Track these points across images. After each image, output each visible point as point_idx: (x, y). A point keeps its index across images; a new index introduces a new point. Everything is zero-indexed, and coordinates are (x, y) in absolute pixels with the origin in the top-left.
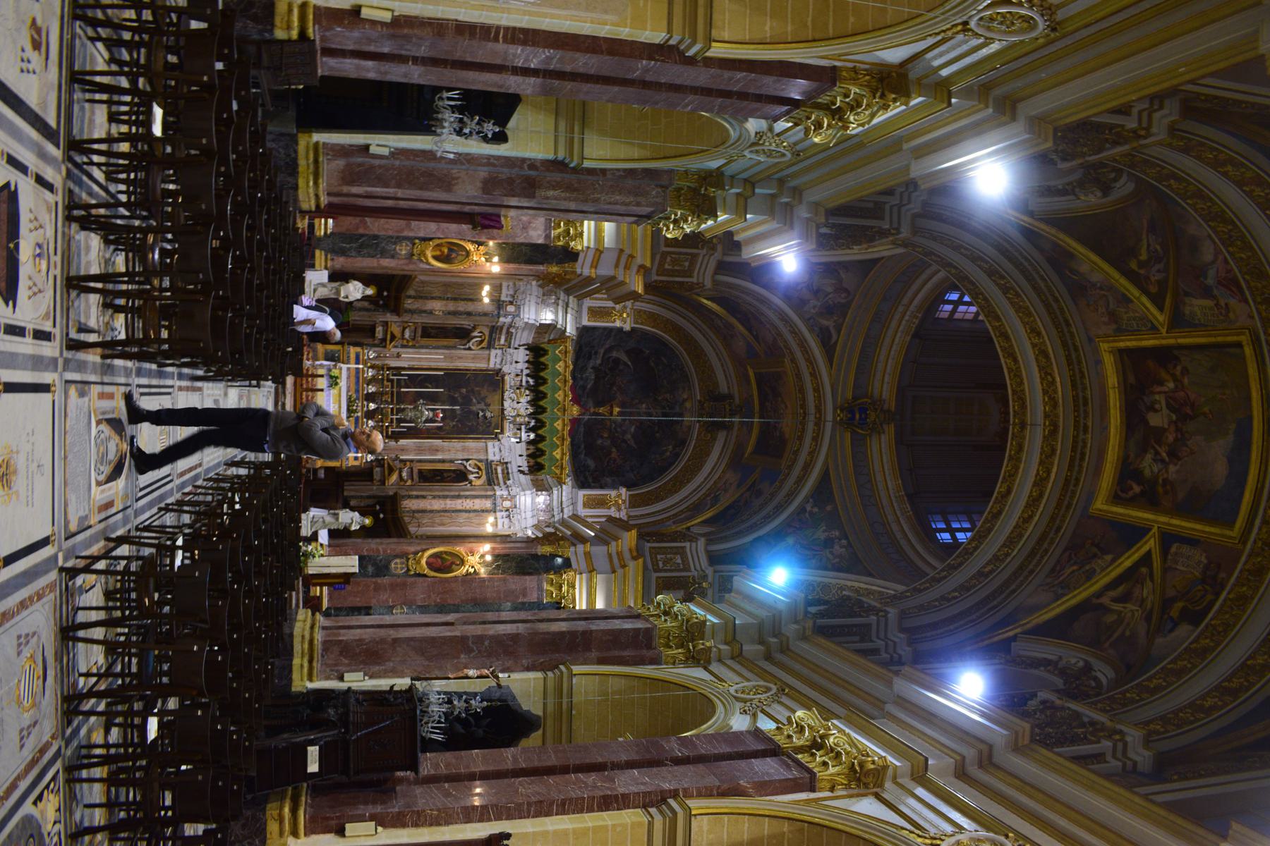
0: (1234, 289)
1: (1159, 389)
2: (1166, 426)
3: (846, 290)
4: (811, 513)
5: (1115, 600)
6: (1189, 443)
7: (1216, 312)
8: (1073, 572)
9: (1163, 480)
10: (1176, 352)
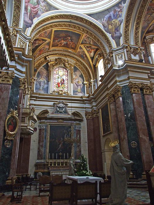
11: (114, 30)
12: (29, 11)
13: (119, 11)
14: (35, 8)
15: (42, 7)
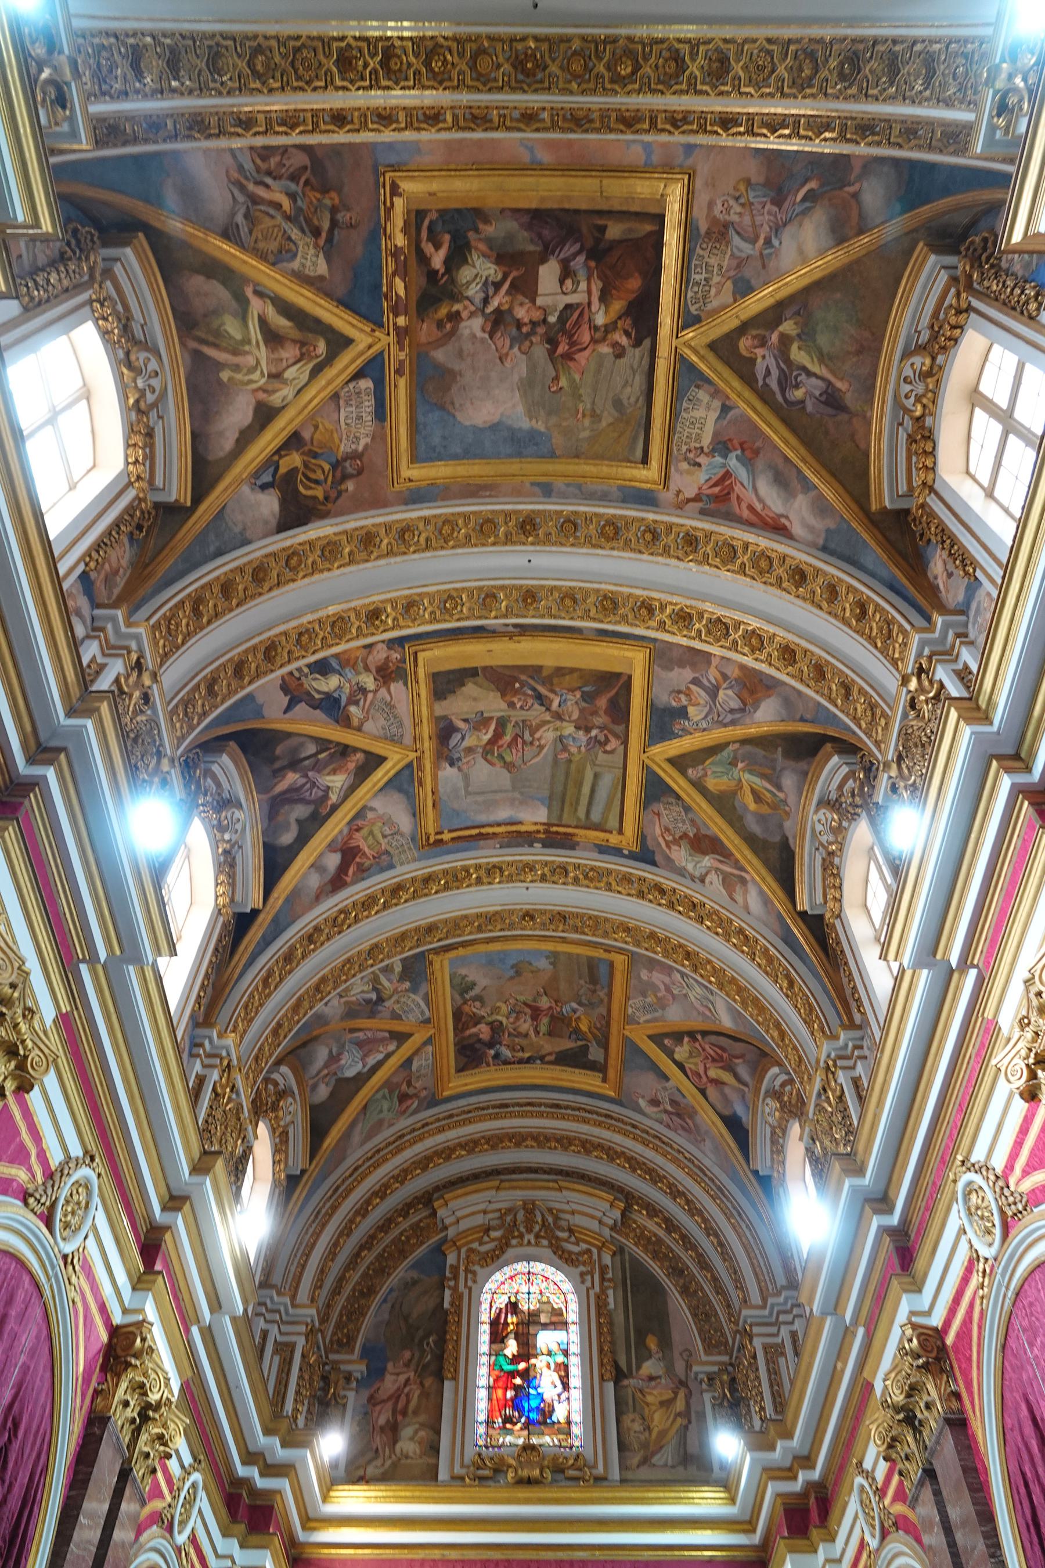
0: (717, 490)
1: (596, 286)
2: (539, 301)
6: (516, 350)
7: (693, 445)
8: (278, 206)
9: (458, 313)
10: (647, 343)
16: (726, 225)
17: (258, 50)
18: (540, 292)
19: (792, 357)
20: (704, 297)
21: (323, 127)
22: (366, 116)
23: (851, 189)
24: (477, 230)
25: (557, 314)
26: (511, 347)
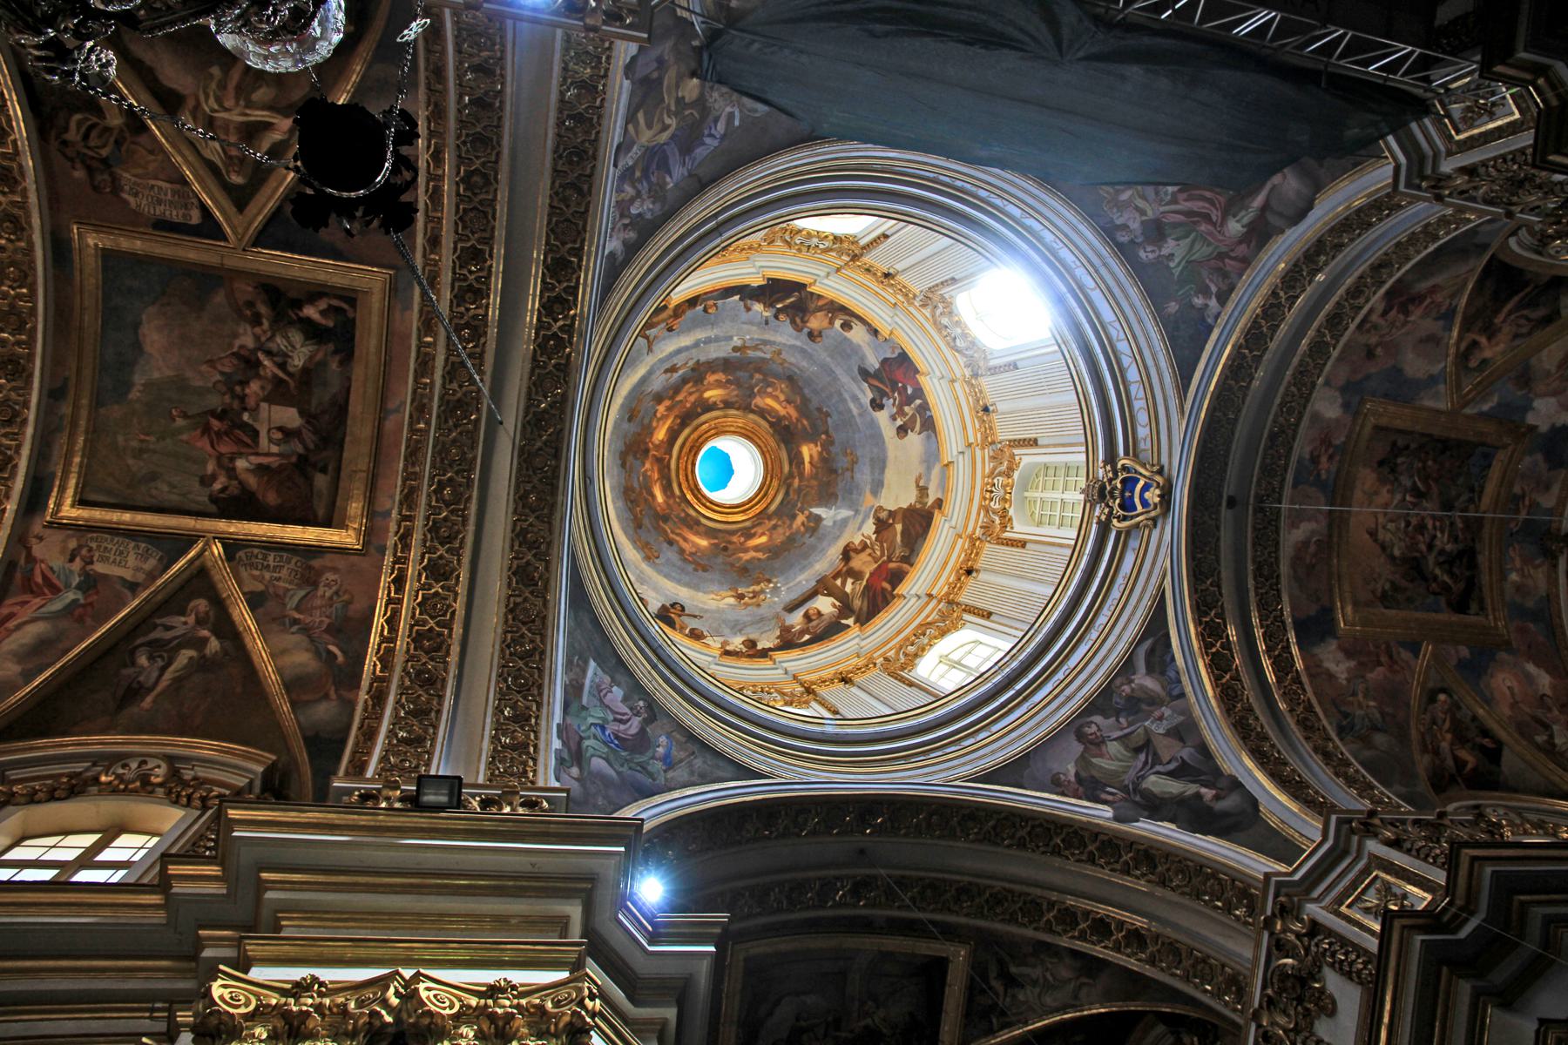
1: (273, 462)
2: (264, 405)
3: (1081, 737)
4: (1206, 292)
5: (268, 126)
6: (218, 377)
9: (260, 324)
10: (213, 508)
11: (670, 77)
12: (1248, 216)
13: (632, 201)
14: (1189, 214)
15: (1141, 203)
16: (315, 584)
17: (488, 183)
18: (275, 408)
19: (183, 651)
20: (251, 565)
21: (429, 226)
22: (435, 265)
23: (333, 694)
24: (335, 352)
25: (251, 422)
26: (222, 373)
